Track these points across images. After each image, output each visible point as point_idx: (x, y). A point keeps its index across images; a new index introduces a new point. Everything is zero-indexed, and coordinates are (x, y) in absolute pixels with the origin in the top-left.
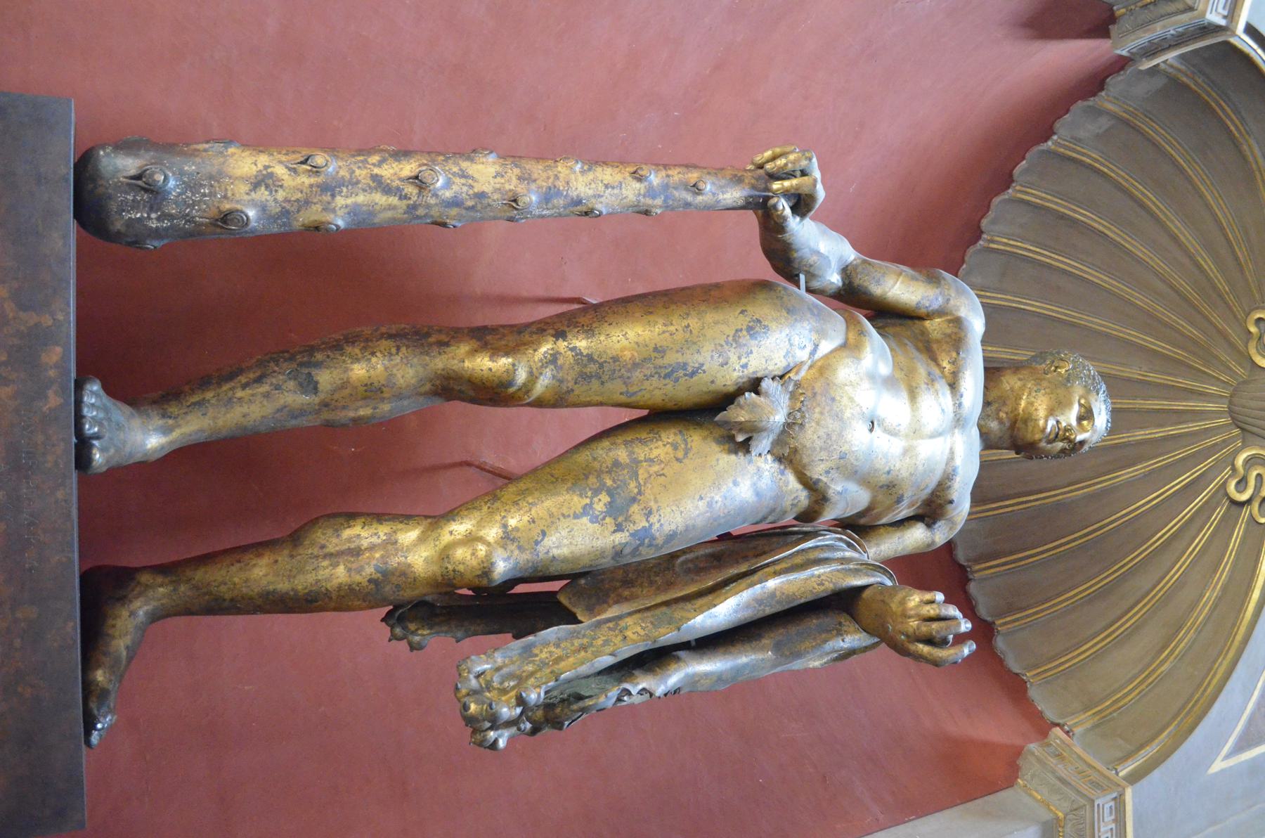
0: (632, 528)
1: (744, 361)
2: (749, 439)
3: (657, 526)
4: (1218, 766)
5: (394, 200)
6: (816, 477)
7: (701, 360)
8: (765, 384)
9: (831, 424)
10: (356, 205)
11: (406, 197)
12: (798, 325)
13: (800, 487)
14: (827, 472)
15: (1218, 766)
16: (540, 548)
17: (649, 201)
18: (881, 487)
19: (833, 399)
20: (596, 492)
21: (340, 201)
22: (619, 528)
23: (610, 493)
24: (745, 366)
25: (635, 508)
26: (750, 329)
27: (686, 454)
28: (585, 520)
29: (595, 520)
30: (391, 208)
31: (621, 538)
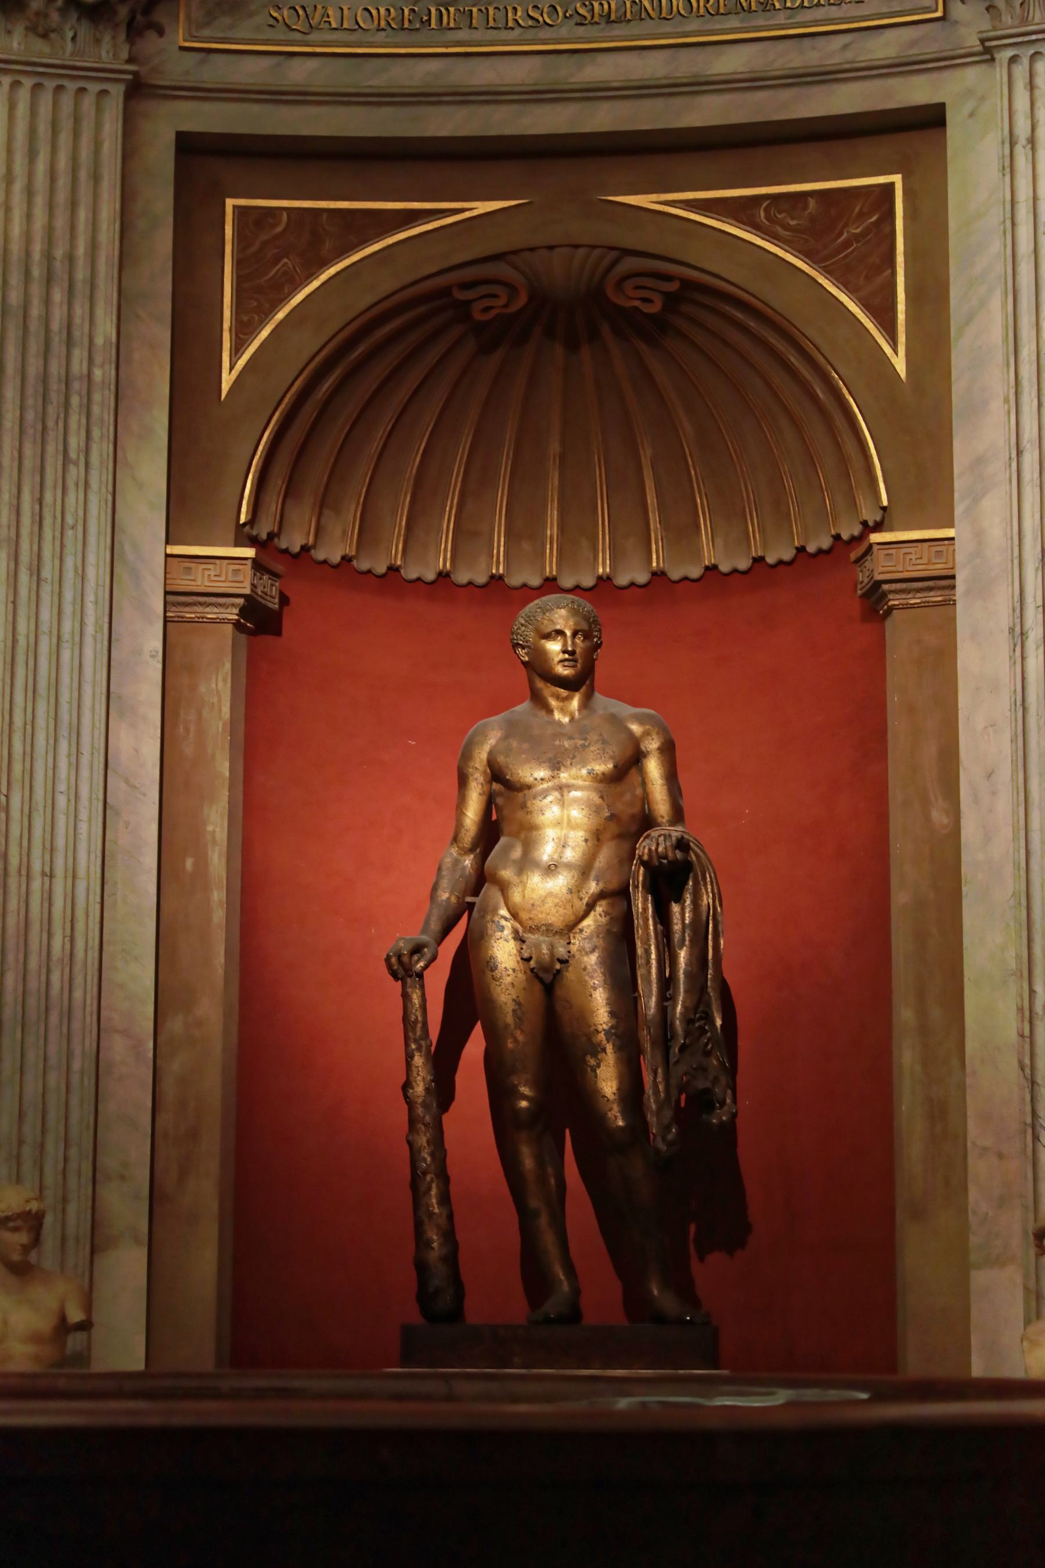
0: (604, 1042)
1: (510, 972)
2: (558, 960)
3: (605, 1026)
4: (900, 364)
5: (434, 1186)
6: (584, 907)
7: (510, 1002)
8: (526, 955)
9: (550, 902)
10: (438, 1203)
11: (432, 1179)
12: (490, 932)
13: (592, 913)
14: (581, 899)
15: (900, 364)
16: (611, 1097)
17: (424, 1049)
18: (598, 840)
19: (533, 905)
20: (585, 1062)
21: (436, 1210)
22: (604, 1050)
23: (586, 1055)
24: (514, 970)
25: (594, 1039)
26: (492, 970)
27: (567, 1001)
28: (598, 1071)
29: (599, 1066)
30: (438, 1187)
31: (609, 1048)
